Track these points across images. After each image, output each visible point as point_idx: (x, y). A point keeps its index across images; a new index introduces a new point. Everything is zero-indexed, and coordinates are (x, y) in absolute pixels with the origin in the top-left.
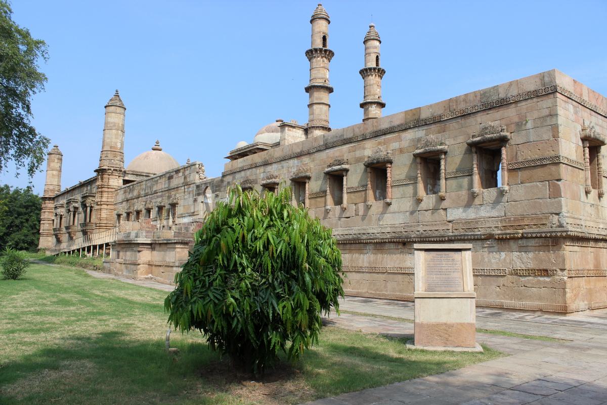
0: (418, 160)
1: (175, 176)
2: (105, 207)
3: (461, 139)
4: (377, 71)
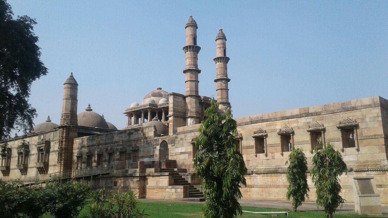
0: (309, 133)
1: (134, 133)
3: (332, 124)
4: (225, 59)
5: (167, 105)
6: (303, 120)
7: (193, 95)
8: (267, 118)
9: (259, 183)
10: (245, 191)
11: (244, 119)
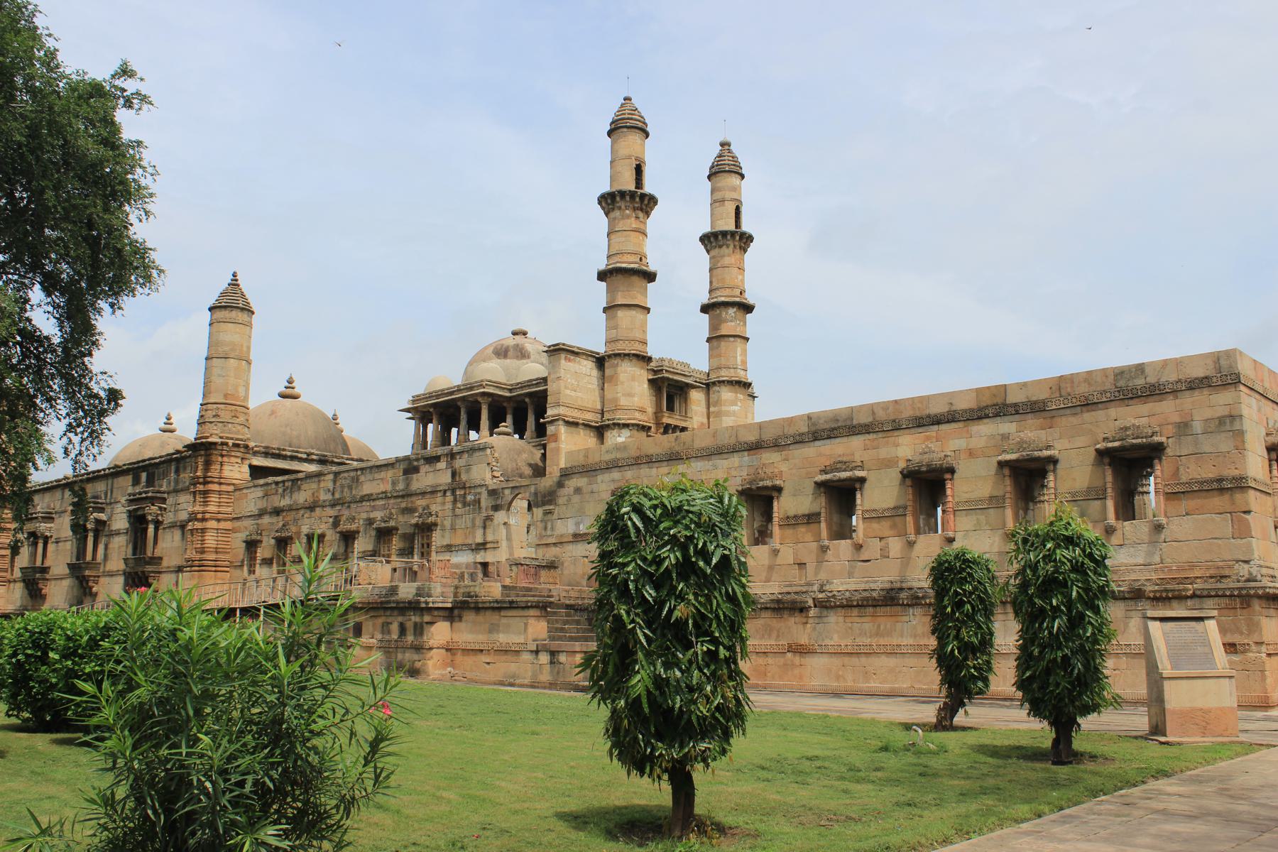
0: (1006, 471)
2: (212, 524)
6: (986, 430)
7: (628, 355)
11: (791, 421)
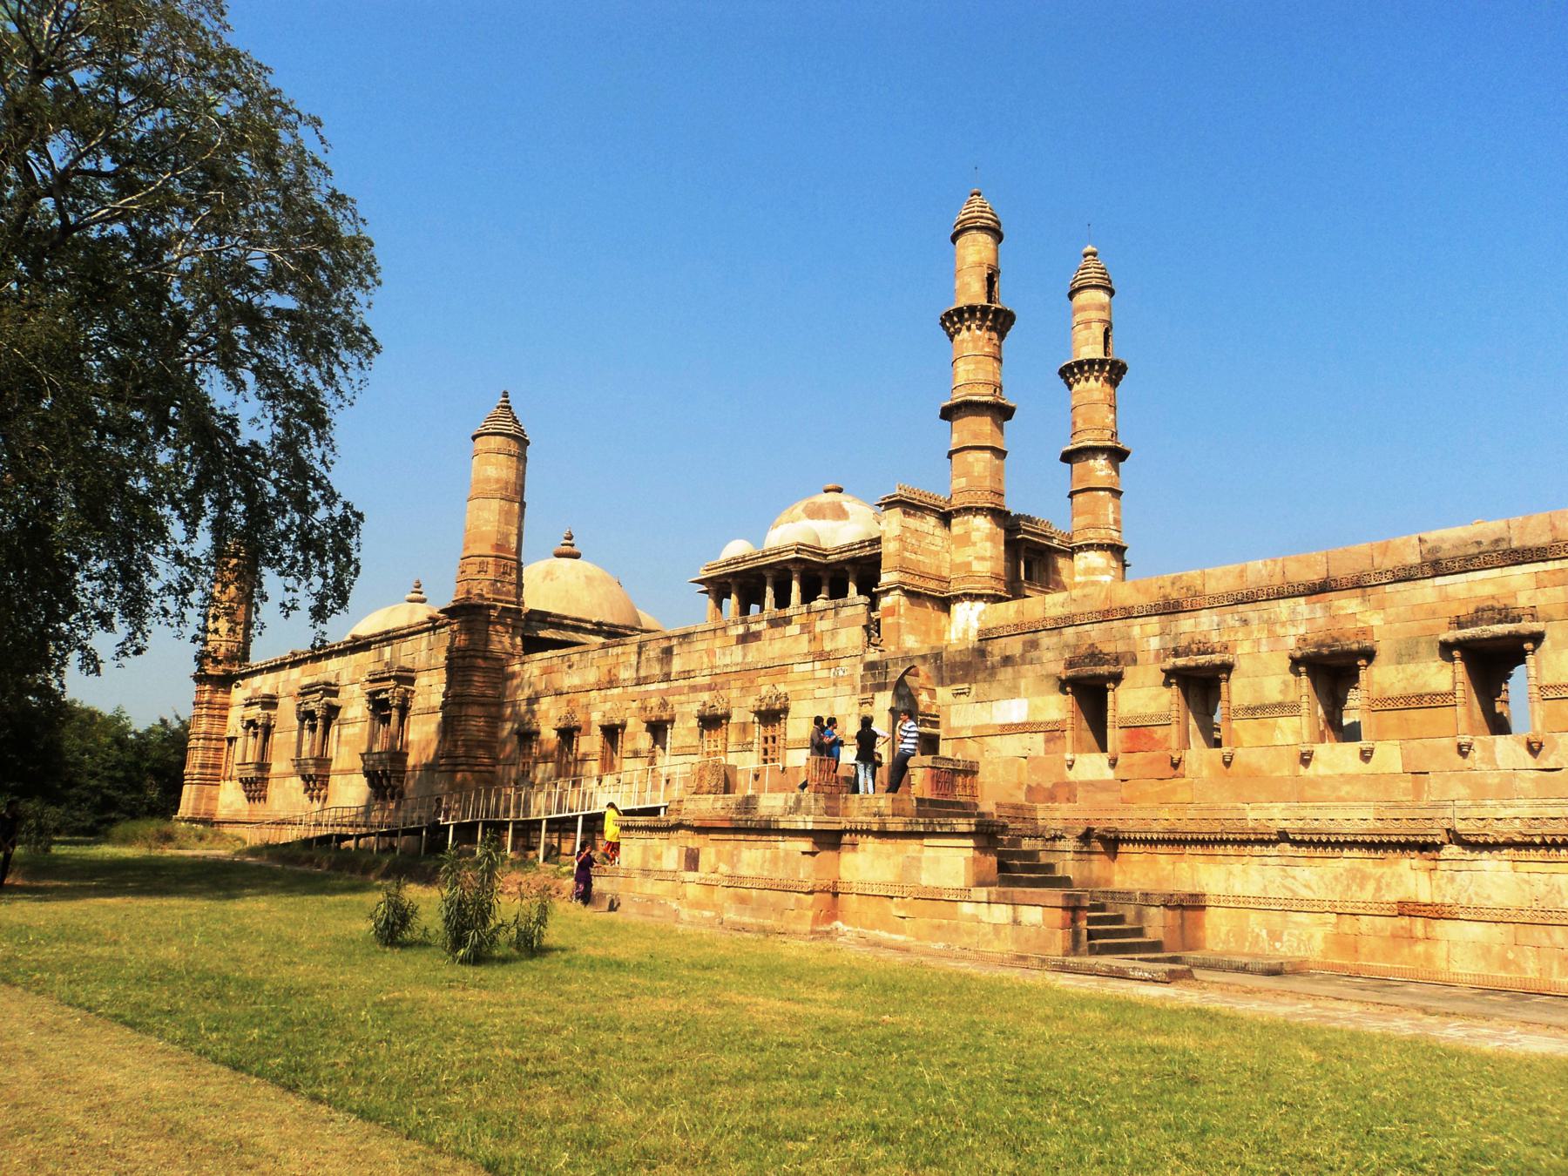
5: (867, 552)
8: (1544, 540)
9: (1489, 898)
10: (1394, 936)
